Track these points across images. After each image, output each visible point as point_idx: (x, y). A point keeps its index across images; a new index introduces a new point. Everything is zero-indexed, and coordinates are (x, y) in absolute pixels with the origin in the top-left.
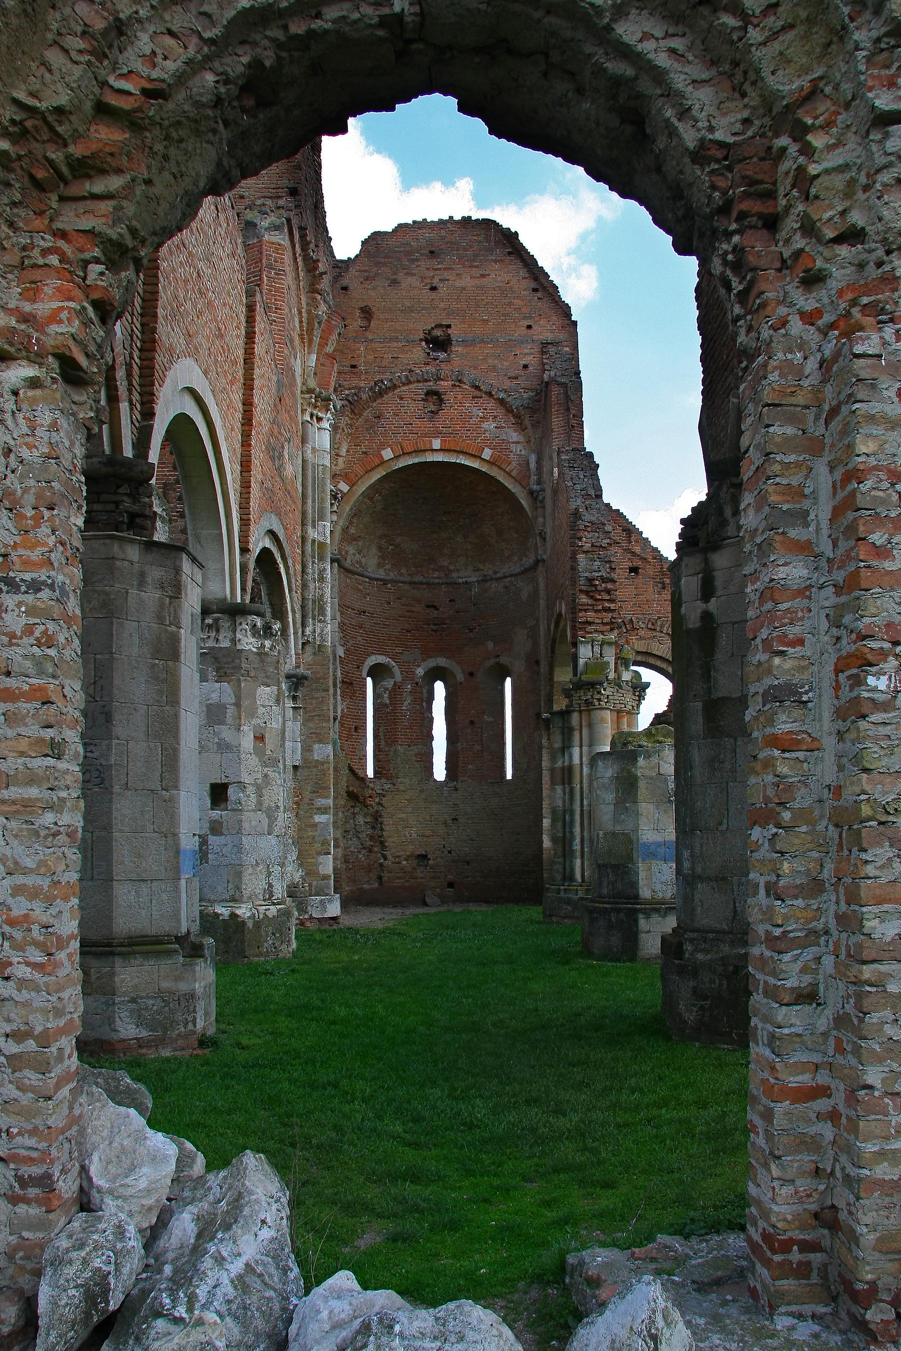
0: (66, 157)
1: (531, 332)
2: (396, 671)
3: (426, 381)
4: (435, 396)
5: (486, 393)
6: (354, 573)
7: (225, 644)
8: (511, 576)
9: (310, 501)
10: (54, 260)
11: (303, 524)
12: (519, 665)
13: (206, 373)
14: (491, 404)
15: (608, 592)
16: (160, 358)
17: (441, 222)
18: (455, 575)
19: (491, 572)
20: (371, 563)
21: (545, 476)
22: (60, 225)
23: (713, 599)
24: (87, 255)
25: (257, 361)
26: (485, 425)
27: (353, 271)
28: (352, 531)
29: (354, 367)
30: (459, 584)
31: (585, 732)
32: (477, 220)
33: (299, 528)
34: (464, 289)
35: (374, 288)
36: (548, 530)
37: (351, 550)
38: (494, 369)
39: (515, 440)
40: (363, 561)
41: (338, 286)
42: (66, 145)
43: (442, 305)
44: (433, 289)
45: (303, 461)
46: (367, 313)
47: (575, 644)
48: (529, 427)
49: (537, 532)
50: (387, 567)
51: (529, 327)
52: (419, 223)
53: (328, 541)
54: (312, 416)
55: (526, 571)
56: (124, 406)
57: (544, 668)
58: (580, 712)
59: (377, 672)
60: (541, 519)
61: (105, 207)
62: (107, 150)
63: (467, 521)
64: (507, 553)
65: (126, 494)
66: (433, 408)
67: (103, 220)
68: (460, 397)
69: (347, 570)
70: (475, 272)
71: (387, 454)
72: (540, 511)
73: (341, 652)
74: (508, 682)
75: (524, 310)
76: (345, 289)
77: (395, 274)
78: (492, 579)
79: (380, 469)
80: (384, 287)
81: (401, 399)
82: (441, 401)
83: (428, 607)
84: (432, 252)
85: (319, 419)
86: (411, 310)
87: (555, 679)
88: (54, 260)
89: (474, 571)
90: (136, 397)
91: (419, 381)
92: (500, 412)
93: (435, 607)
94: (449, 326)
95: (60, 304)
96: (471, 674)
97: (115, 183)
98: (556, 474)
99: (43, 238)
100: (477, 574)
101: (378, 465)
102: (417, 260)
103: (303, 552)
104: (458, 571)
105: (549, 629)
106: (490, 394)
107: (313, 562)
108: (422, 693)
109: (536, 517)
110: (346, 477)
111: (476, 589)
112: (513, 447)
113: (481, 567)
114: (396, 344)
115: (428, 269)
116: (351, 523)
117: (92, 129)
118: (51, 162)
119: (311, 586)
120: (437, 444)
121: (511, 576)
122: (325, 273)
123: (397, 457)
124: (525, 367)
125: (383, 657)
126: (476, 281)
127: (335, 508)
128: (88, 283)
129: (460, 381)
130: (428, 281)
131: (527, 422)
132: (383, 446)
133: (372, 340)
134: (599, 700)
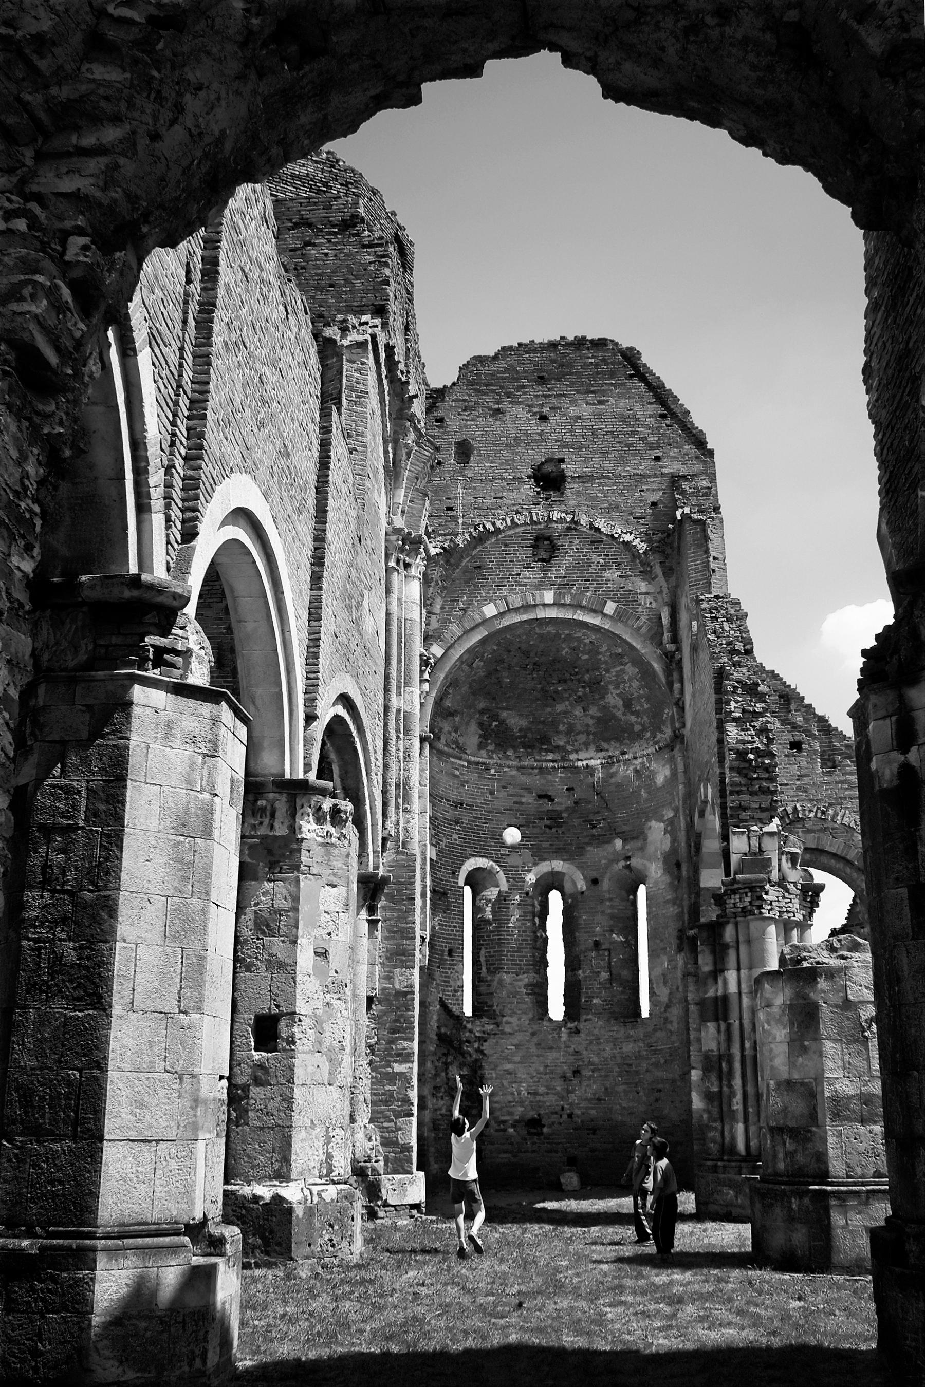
0: (46, 101)
2: (502, 877)
7: (281, 830)
9: (394, 662)
10: (21, 225)
13: (266, 496)
16: (208, 468)
17: (553, 345)
18: (573, 757)
21: (684, 634)
22: (35, 188)
23: (914, 749)
24: (68, 224)
25: (331, 490)
26: (607, 574)
28: (448, 703)
29: (450, 509)
31: (743, 948)
33: (381, 695)
37: (446, 726)
39: (644, 590)
42: (47, 87)
44: (544, 418)
48: (660, 574)
50: (490, 748)
51: (657, 459)
52: (526, 345)
56: (157, 520)
59: (476, 880)
61: (95, 165)
62: (101, 91)
64: (637, 728)
65: (155, 625)
66: (544, 555)
67: (92, 180)
69: (440, 752)
72: (676, 675)
73: (431, 853)
74: (642, 891)
75: (652, 439)
76: (441, 420)
78: (618, 761)
81: (506, 545)
83: (540, 797)
84: (541, 378)
85: (407, 566)
87: (702, 885)
88: (21, 225)
90: (176, 513)
92: (625, 558)
93: (551, 799)
94: (562, 461)
95: (22, 277)
96: (595, 882)
97: (111, 134)
98: (695, 629)
99: (9, 200)
102: (523, 387)
104: (577, 752)
107: (398, 737)
108: (533, 905)
109: (670, 685)
111: (599, 774)
117: (83, 69)
118: (25, 105)
119: (394, 766)
122: (416, 396)
127: (426, 676)
128: (67, 258)
131: (658, 570)
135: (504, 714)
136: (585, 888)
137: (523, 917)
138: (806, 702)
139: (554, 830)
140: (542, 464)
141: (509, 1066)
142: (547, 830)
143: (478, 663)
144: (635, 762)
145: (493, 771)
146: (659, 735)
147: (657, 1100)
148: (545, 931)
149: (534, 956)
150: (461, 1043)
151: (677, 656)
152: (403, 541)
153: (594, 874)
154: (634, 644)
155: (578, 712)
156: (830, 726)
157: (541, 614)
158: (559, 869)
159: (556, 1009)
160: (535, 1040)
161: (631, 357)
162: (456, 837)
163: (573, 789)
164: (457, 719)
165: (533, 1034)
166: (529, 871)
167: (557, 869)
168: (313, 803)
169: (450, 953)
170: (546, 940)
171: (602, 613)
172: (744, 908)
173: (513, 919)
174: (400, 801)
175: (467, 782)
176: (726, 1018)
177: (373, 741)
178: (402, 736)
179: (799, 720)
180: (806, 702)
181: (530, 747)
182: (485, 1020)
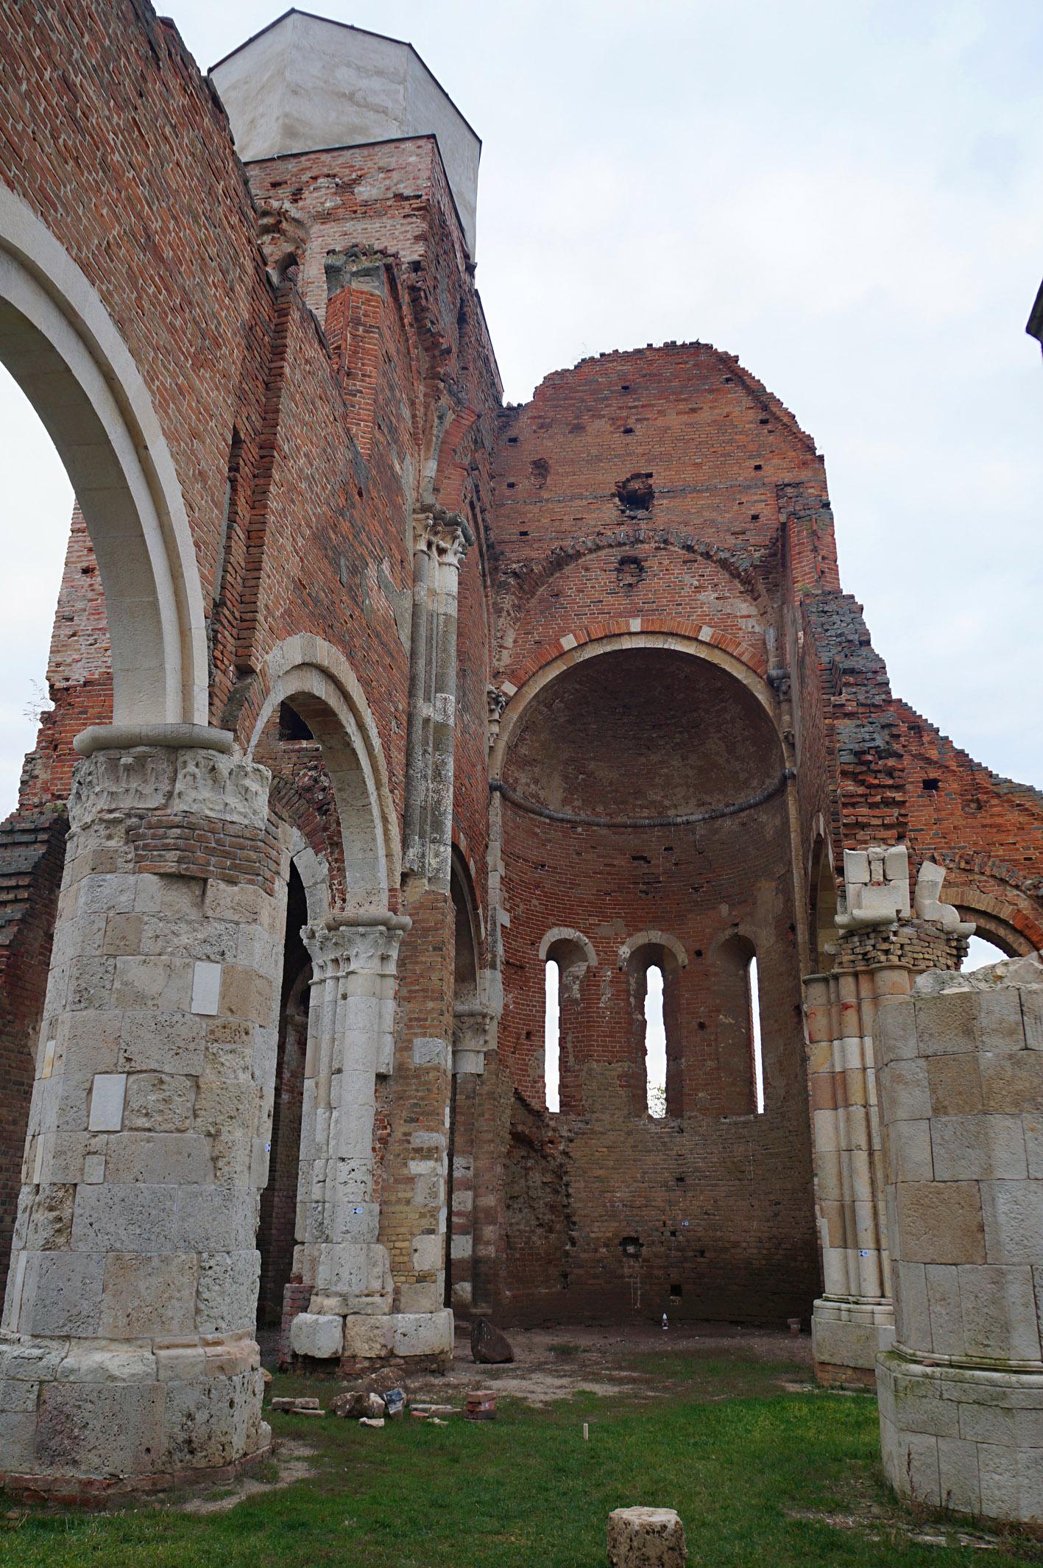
1: (761, 473)
2: (590, 950)
3: (620, 545)
4: (633, 564)
5: (702, 554)
6: (527, 810)
8: (750, 807)
9: (422, 662)
11: (411, 694)
12: (765, 937)
14: (710, 569)
15: (890, 773)
17: (638, 351)
18: (671, 812)
19: (721, 806)
20: (553, 797)
26: (702, 596)
27: (524, 419)
28: (523, 750)
29: (525, 534)
30: (676, 825)
31: (867, 1008)
32: (684, 345)
34: (669, 428)
35: (551, 438)
36: (797, 731)
38: (713, 521)
39: (744, 613)
40: (542, 794)
41: (505, 437)
43: (640, 450)
44: (628, 431)
45: (415, 605)
46: (541, 467)
47: (840, 871)
49: (781, 736)
50: (576, 803)
51: (758, 468)
53: (451, 722)
54: (430, 545)
55: (770, 797)
57: (802, 935)
58: (856, 975)
59: (561, 952)
60: (786, 718)
63: (686, 736)
64: (743, 776)
66: (629, 580)
68: (666, 562)
69: (517, 805)
71: (568, 642)
72: (785, 706)
75: (751, 447)
76: (513, 440)
77: (577, 417)
78: (723, 815)
79: (559, 662)
81: (587, 570)
82: (641, 569)
83: (634, 858)
84: (625, 388)
85: (442, 551)
86: (598, 459)
89: (699, 806)
91: (610, 546)
92: (723, 576)
93: (644, 859)
94: (650, 475)
96: (699, 953)
100: (702, 809)
101: (556, 658)
102: (607, 398)
103: (409, 734)
104: (676, 807)
105: (805, 869)
106: (707, 555)
107: (425, 751)
108: (628, 983)
109: (779, 717)
110: (513, 676)
111: (701, 830)
112: (742, 623)
113: (708, 799)
114: (578, 502)
115: (620, 408)
116: (522, 739)
120: (636, 625)
121: (750, 807)
123: (581, 646)
124: (755, 517)
125: (571, 931)
126: (685, 418)
127: (496, 716)
129: (665, 542)
130: (619, 423)
131: (761, 587)
132: (563, 632)
133: (547, 500)
134: (887, 952)
135: (592, 766)
136: (687, 962)
137: (616, 996)
138: (941, 734)
139: (650, 896)
140: (628, 480)
141: (600, 1172)
142: (643, 895)
143: (558, 704)
144: (742, 814)
145: (580, 830)
146: (768, 781)
147: (776, 1215)
148: (643, 1014)
149: (628, 1041)
150: (543, 1144)
151: (784, 688)
152: (435, 518)
153: (697, 946)
154: (735, 674)
155: (676, 763)
156: (971, 760)
157: (627, 644)
158: (658, 941)
159: (656, 1106)
160: (631, 1141)
161: (727, 363)
162: (535, 902)
163: (671, 849)
164: (537, 770)
165: (629, 1133)
166: (623, 943)
167: (654, 941)
168: (203, 762)
169: (529, 1035)
170: (644, 1023)
171: (696, 639)
172: (865, 954)
173: (604, 998)
174: (428, 828)
175: (550, 841)
176: (847, 1105)
177: (386, 748)
178: (430, 750)
179: (933, 754)
180: (941, 734)
181: (622, 803)
182: (573, 1117)
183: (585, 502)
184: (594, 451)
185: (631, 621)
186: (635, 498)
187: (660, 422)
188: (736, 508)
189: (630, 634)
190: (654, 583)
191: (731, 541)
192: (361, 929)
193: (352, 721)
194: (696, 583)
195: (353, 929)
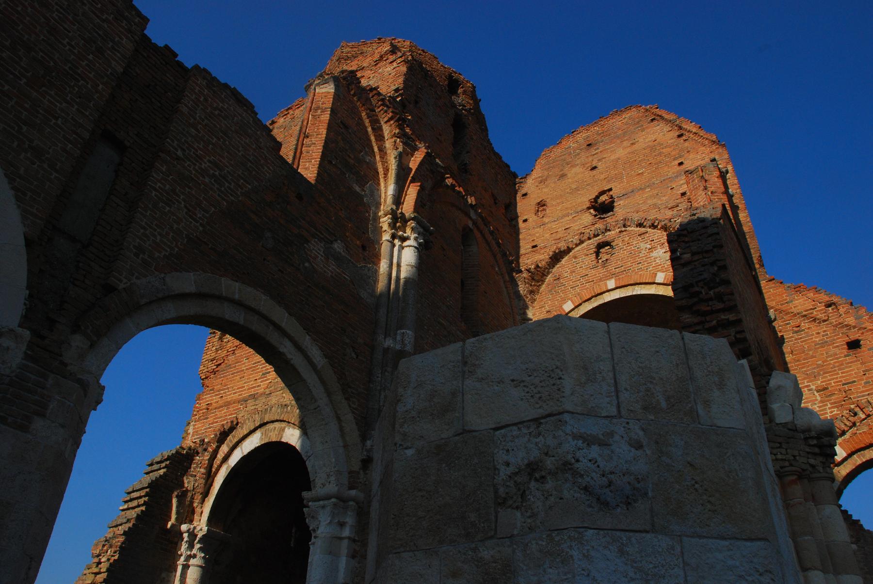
3: (596, 236)
5: (650, 227)
15: (720, 297)
26: (654, 254)
35: (547, 186)
38: (655, 205)
43: (602, 177)
44: (594, 168)
51: (681, 164)
70: (626, 144)
75: (673, 153)
76: (525, 195)
80: (555, 182)
81: (575, 258)
82: (612, 247)
84: (589, 145)
85: (404, 239)
86: (577, 189)
91: (589, 239)
94: (610, 190)
102: (578, 154)
106: (653, 226)
124: (683, 194)
126: (629, 150)
129: (624, 226)
132: (564, 301)
140: (597, 197)
157: (608, 298)
178: (389, 369)
183: (570, 217)
184: (574, 186)
185: (608, 282)
186: (602, 207)
187: (612, 158)
188: (670, 191)
189: (608, 291)
190: (621, 253)
191: (669, 213)
192: (321, 503)
193: (288, 343)
194: (649, 246)
195: (317, 503)
